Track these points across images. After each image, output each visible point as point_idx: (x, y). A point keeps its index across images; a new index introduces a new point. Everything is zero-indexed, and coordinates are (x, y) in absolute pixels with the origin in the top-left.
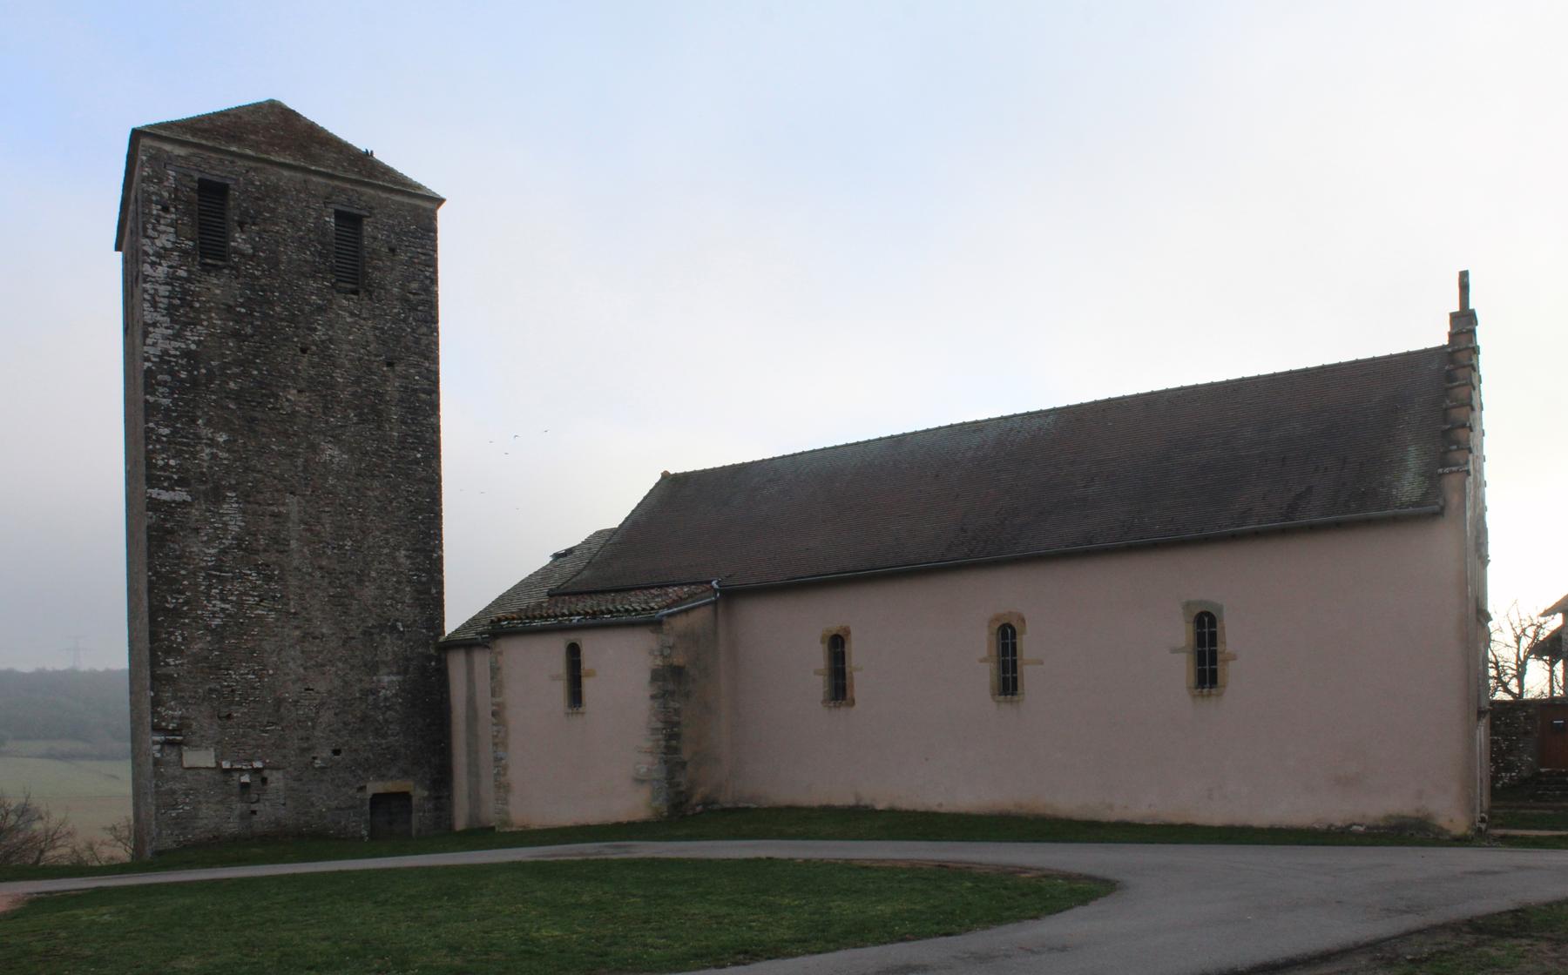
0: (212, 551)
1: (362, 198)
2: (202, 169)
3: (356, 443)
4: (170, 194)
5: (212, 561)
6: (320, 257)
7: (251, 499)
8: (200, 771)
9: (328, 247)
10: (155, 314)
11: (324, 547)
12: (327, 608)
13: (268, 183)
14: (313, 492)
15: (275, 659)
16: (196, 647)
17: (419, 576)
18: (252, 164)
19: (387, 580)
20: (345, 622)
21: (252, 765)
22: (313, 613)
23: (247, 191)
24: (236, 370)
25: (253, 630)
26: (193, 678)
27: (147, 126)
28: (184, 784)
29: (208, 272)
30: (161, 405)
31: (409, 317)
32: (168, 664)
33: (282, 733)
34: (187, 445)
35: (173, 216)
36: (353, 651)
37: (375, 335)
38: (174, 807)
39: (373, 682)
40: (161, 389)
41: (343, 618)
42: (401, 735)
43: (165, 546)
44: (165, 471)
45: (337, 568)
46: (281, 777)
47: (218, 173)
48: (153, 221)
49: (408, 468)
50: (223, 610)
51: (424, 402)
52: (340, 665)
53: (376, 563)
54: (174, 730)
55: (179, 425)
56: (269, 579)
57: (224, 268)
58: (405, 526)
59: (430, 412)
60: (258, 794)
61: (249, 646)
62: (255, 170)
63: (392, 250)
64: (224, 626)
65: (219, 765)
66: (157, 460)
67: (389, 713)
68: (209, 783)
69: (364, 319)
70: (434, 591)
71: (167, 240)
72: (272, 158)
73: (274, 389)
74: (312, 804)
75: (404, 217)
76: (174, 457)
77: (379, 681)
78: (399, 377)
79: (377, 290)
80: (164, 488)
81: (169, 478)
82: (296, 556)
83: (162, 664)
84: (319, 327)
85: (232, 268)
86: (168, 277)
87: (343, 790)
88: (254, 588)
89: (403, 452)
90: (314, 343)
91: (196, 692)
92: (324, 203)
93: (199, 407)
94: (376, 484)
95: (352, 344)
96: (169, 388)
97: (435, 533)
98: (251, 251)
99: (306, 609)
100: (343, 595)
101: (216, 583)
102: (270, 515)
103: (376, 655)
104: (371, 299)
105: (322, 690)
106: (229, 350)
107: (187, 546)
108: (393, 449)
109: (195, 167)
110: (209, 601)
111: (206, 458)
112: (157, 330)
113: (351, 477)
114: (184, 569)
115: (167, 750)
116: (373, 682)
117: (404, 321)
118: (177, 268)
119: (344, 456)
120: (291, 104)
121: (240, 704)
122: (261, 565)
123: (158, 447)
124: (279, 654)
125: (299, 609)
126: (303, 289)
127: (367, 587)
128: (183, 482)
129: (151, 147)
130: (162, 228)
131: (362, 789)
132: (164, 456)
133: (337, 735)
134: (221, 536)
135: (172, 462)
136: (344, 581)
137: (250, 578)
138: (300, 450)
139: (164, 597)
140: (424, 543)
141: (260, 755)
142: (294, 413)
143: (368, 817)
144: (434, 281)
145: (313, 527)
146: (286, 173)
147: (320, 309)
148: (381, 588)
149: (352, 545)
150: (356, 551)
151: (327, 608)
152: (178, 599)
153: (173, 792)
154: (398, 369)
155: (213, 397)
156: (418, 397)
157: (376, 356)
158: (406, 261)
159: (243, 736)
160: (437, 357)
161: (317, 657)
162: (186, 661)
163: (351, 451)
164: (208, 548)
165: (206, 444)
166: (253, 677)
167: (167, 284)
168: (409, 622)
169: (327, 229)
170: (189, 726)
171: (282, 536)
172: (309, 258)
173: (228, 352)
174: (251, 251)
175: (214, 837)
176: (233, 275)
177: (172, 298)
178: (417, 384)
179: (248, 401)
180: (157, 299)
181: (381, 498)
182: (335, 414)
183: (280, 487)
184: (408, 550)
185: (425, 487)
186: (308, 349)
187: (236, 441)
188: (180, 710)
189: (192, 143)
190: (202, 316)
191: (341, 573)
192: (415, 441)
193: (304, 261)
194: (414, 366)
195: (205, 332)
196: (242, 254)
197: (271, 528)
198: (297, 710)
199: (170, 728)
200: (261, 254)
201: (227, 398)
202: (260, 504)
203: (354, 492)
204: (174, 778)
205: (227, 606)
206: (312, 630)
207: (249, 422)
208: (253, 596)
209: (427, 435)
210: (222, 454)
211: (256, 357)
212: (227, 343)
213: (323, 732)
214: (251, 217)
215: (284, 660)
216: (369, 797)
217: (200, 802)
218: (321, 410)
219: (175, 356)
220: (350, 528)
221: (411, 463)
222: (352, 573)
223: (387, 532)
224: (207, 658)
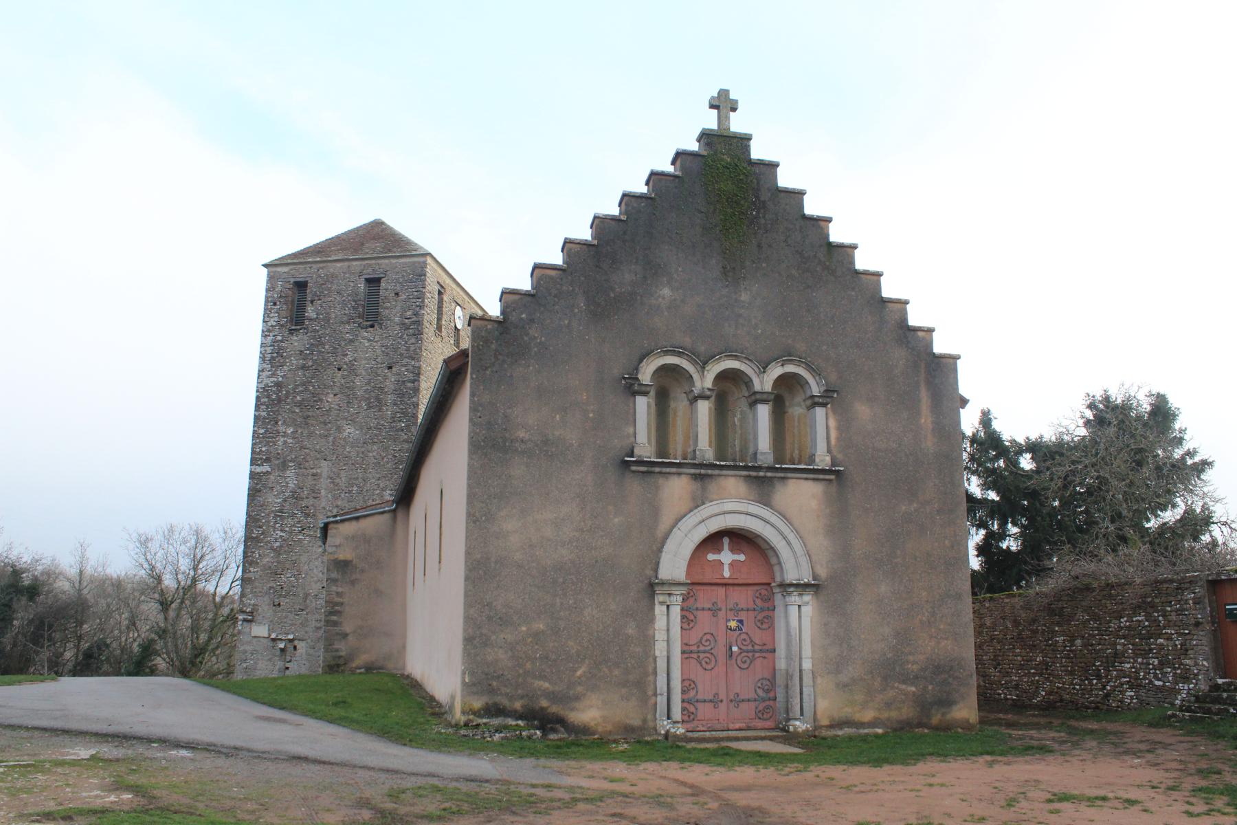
0: (279, 500)
6: (354, 309)
7: (302, 466)
9: (358, 302)
11: (340, 493)
16: (266, 560)
18: (321, 265)
23: (317, 282)
27: (271, 262)
29: (292, 334)
32: (250, 572)
34: (272, 437)
35: (278, 307)
37: (382, 351)
43: (255, 500)
45: (347, 505)
49: (396, 435)
50: (281, 536)
53: (370, 501)
54: (249, 612)
56: (307, 515)
59: (413, 395)
61: (293, 558)
62: (322, 268)
63: (397, 294)
64: (281, 546)
65: (270, 635)
69: (376, 342)
75: (406, 271)
76: (265, 446)
78: (395, 375)
80: (259, 465)
81: (261, 459)
84: (349, 353)
85: (305, 328)
91: (263, 589)
92: (359, 276)
94: (375, 447)
95: (369, 359)
96: (266, 405)
102: (312, 475)
104: (381, 328)
107: (266, 499)
108: (387, 423)
112: (264, 373)
113: (360, 445)
114: (264, 512)
117: (400, 338)
123: (258, 441)
128: (268, 460)
146: (339, 265)
147: (351, 341)
153: (246, 652)
154: (394, 369)
155: (288, 407)
157: (382, 364)
158: (405, 299)
163: (362, 429)
167: (271, 346)
170: (257, 611)
171: (317, 488)
172: (346, 312)
174: (315, 316)
179: (306, 406)
180: (266, 355)
181: (377, 457)
183: (318, 456)
184: (392, 490)
187: (297, 431)
194: (405, 366)
196: (310, 319)
197: (311, 483)
198: (316, 601)
200: (321, 316)
202: (306, 469)
203: (361, 455)
204: (249, 643)
205: (284, 534)
207: (304, 418)
208: (298, 527)
210: (290, 441)
217: (258, 659)
219: (271, 386)
220: (357, 479)
223: (379, 479)
224: (270, 567)
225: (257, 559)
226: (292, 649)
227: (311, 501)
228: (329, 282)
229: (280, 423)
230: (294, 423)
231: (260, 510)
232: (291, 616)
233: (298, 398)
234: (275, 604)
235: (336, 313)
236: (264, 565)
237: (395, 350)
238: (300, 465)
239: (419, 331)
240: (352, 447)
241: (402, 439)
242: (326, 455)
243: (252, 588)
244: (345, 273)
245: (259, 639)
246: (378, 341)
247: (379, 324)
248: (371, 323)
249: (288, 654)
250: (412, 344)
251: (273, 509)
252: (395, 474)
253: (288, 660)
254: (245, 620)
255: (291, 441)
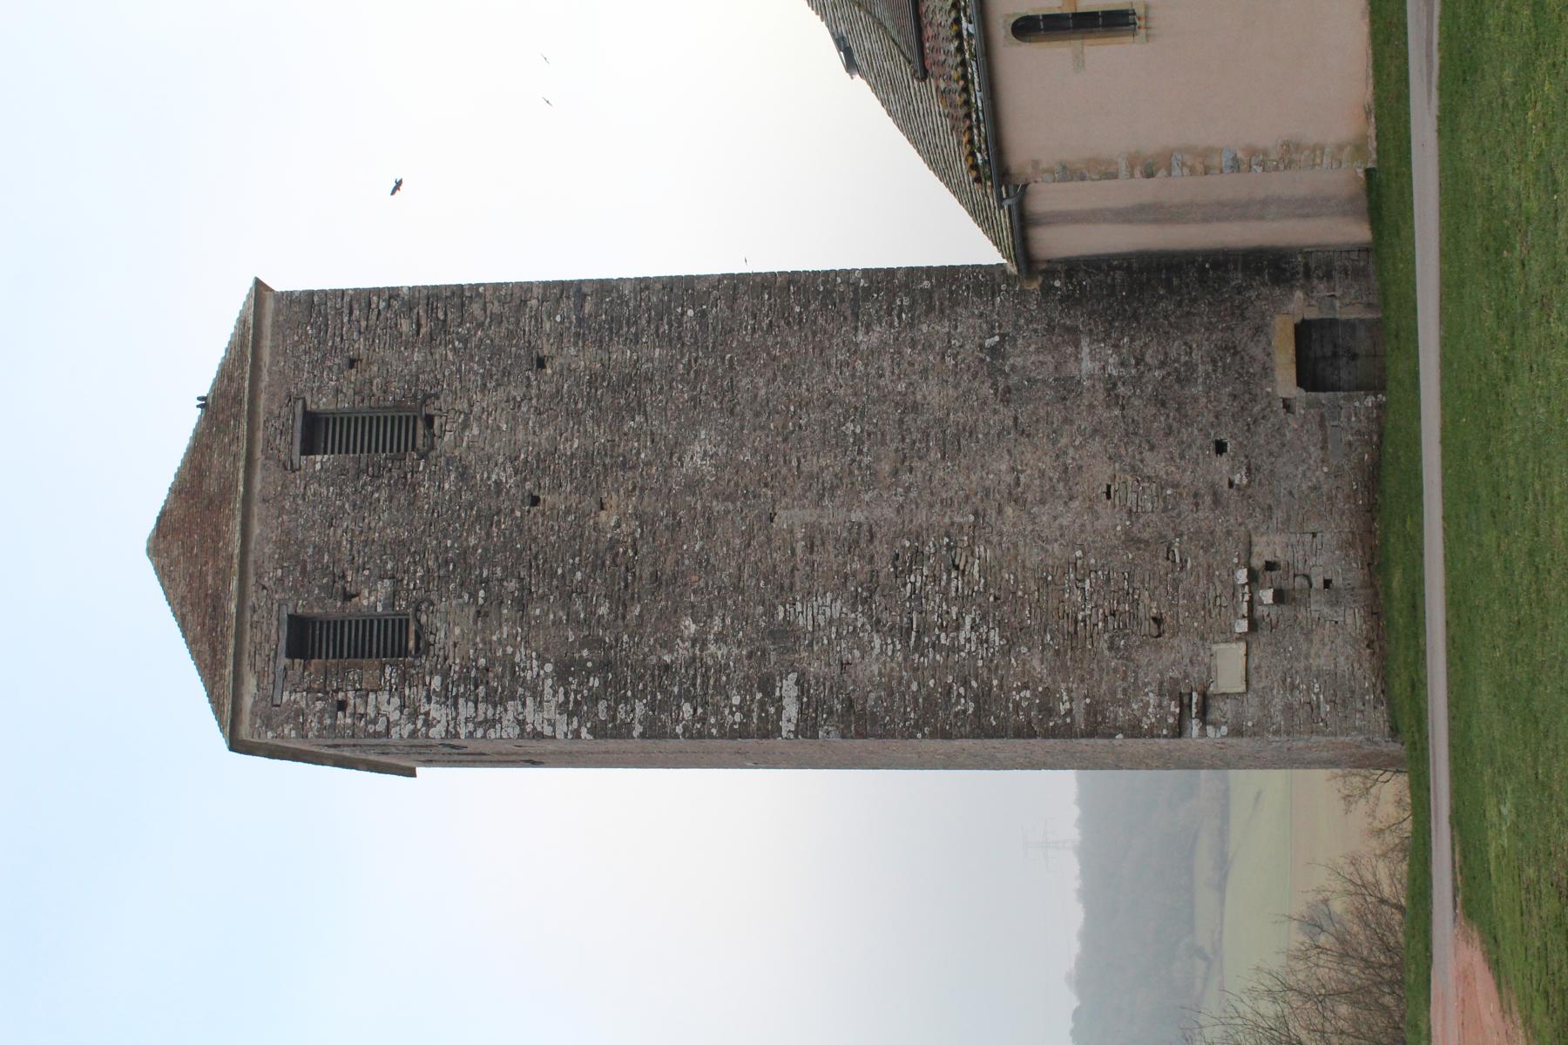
0: (877, 642)
1: (276, 412)
2: (272, 654)
3: (679, 417)
4: (318, 699)
5: (893, 642)
7: (787, 582)
8: (1252, 665)
9: (363, 465)
10: (505, 723)
11: (860, 468)
12: (964, 462)
13: (276, 556)
14: (766, 485)
15: (1056, 545)
17: (901, 311)
18: (252, 580)
19: (911, 364)
20: (989, 433)
21: (1243, 586)
22: (974, 486)
23: (294, 588)
24: (578, 605)
25: (1008, 581)
26: (1092, 676)
27: (222, 730)
28: (1275, 691)
29: (429, 645)
30: (646, 716)
31: (458, 333)
32: (1069, 712)
33: (1186, 538)
34: (705, 676)
35: (351, 694)
36: (1038, 421)
38: (1313, 707)
39: (1094, 386)
40: (621, 715)
41: (980, 436)
42: (1189, 338)
43: (873, 713)
44: (751, 711)
45: (893, 446)
46: (1265, 539)
47: (273, 631)
48: (363, 723)
49: (714, 329)
51: (597, 305)
52: (1064, 441)
53: (882, 382)
54: (1181, 705)
55: (676, 690)
56: (918, 556)
57: (419, 621)
58: (814, 334)
59: (615, 295)
60: (1295, 576)
61: (1034, 587)
62: (259, 576)
63: (352, 363)
65: (1241, 637)
66: (734, 723)
67: (1148, 359)
68: (1274, 654)
69: (471, 406)
70: (926, 284)
71: (389, 703)
72: (237, 551)
73: (602, 547)
74: (1315, 488)
75: (295, 345)
76: (728, 698)
77: (1091, 377)
79: (421, 386)
81: (762, 704)
82: (877, 513)
83: (1068, 720)
84: (494, 477)
85: (417, 609)
86: (444, 703)
87: (1289, 435)
88: (936, 579)
89: (688, 340)
90: (520, 485)
91: (1115, 670)
92: (294, 471)
93: (644, 659)
94: (744, 382)
96: (617, 704)
97: (824, 283)
98: (387, 582)
99: (967, 497)
100: (940, 436)
101: (929, 637)
102: (811, 552)
103: (1044, 382)
105: (1110, 472)
106: (547, 614)
108: (683, 356)
109: (271, 663)
110: (960, 650)
111: (725, 650)
113: (737, 424)
115: (1214, 715)
116: (1094, 386)
118: (429, 690)
119: (703, 437)
120: (150, 524)
121: (1136, 603)
122: (896, 568)
123: (713, 720)
124: (1047, 541)
125: (968, 508)
126: (436, 503)
127: (924, 397)
128: (767, 685)
129: (252, 725)
130: (371, 712)
131: (1287, 406)
132: (727, 712)
133: (1190, 446)
134: (851, 628)
135: (736, 700)
136: (917, 436)
137: (918, 584)
138: (699, 507)
139: (957, 714)
140: (842, 300)
141: (1225, 574)
142: (636, 515)
143: (1341, 394)
144: (393, 294)
145: (827, 485)
146: (256, 529)
147: (463, 475)
148: (924, 373)
149: (853, 421)
150: (862, 415)
151: (964, 462)
152: (959, 695)
153: (1289, 709)
155: (625, 638)
156: (590, 315)
157: (529, 386)
159: (1192, 597)
160: (520, 285)
161: (1051, 479)
162: (1063, 686)
163: (693, 424)
164: (872, 648)
165: (702, 650)
166: (1088, 581)
167: (455, 705)
168: (984, 326)
169: (334, 468)
170: (1175, 681)
171: (845, 534)
172: (384, 494)
173: (551, 616)
174: (387, 582)
175: (1368, 646)
176: (428, 608)
177: (477, 695)
178: (569, 318)
179: (626, 586)
180: (481, 718)
181: (770, 374)
182: (634, 451)
184: (856, 328)
185: (744, 302)
186: (531, 494)
187: (693, 606)
188: (1147, 694)
189: (234, 666)
190: (499, 653)
191: (903, 440)
192: (665, 321)
193: (391, 501)
194: (537, 318)
195: (522, 649)
198: (1145, 512)
199: (1178, 710)
200: (389, 566)
201: (624, 617)
202: (794, 569)
204: (1264, 706)
205: (968, 620)
206: (1003, 487)
209: (654, 299)
211: (553, 574)
212: (536, 618)
213: (1184, 471)
214: (334, 582)
215: (1058, 533)
216: (1303, 392)
218: (630, 474)
219: (566, 694)
220: (824, 425)
221: (704, 326)
222: (901, 421)
225: (1034, 695)
226: (1274, 573)
227: (881, 548)
228: (298, 554)
229: (667, 658)
230: (670, 617)
231: (903, 695)
232: (1187, 582)
233: (603, 610)
234: (1155, 633)
235: (383, 524)
236: (1051, 671)
237: (497, 352)
238: (782, 588)
239: (453, 294)
240: (742, 445)
241: (727, 313)
242: (759, 517)
243: (1115, 701)
244: (282, 509)
245: (1252, 671)
246: (469, 400)
247: (424, 401)
248: (420, 424)
249: (1287, 585)
250: (485, 310)
251: (899, 656)
252: (814, 322)
253: (1306, 583)
254: (1203, 713)
255: (717, 620)
